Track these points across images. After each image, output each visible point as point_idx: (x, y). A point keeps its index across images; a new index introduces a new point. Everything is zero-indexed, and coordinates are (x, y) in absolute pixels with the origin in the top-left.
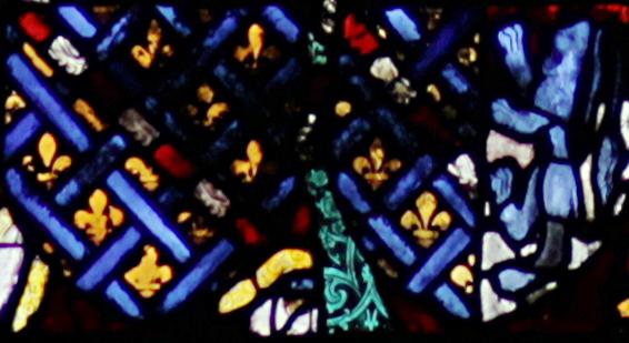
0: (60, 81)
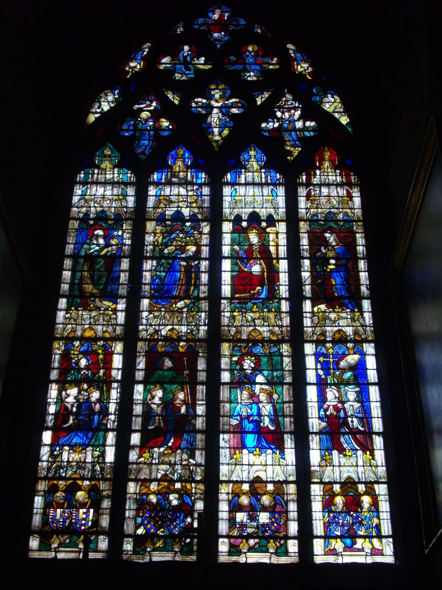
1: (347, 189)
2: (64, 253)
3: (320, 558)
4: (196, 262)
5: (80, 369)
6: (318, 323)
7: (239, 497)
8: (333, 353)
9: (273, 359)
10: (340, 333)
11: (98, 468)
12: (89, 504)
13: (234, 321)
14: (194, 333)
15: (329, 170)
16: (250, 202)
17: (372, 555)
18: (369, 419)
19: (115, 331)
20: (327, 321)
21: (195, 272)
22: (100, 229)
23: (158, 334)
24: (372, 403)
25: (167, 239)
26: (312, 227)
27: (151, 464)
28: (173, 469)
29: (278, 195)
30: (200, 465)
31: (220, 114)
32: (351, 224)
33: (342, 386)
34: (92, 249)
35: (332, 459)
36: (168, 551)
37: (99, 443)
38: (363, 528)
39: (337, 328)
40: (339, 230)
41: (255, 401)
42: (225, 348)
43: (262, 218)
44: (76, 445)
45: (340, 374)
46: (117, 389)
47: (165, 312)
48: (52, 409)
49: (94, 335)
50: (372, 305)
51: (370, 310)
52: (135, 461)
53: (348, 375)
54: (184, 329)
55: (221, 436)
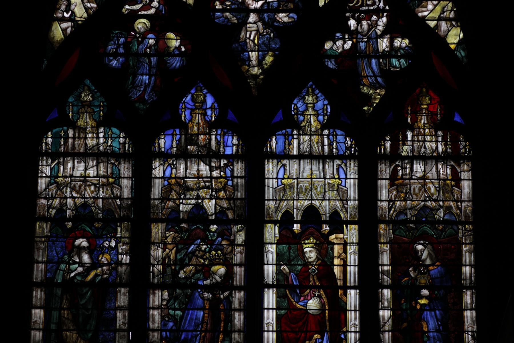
1: (452, 166)
2: (32, 278)
4: (226, 294)
15: (427, 131)
16: (306, 189)
21: (224, 310)
22: (83, 238)
25: (183, 253)
26: (397, 233)
29: (348, 177)
31: (260, 24)
32: (455, 228)
34: (72, 272)
40: (437, 238)
43: (323, 217)
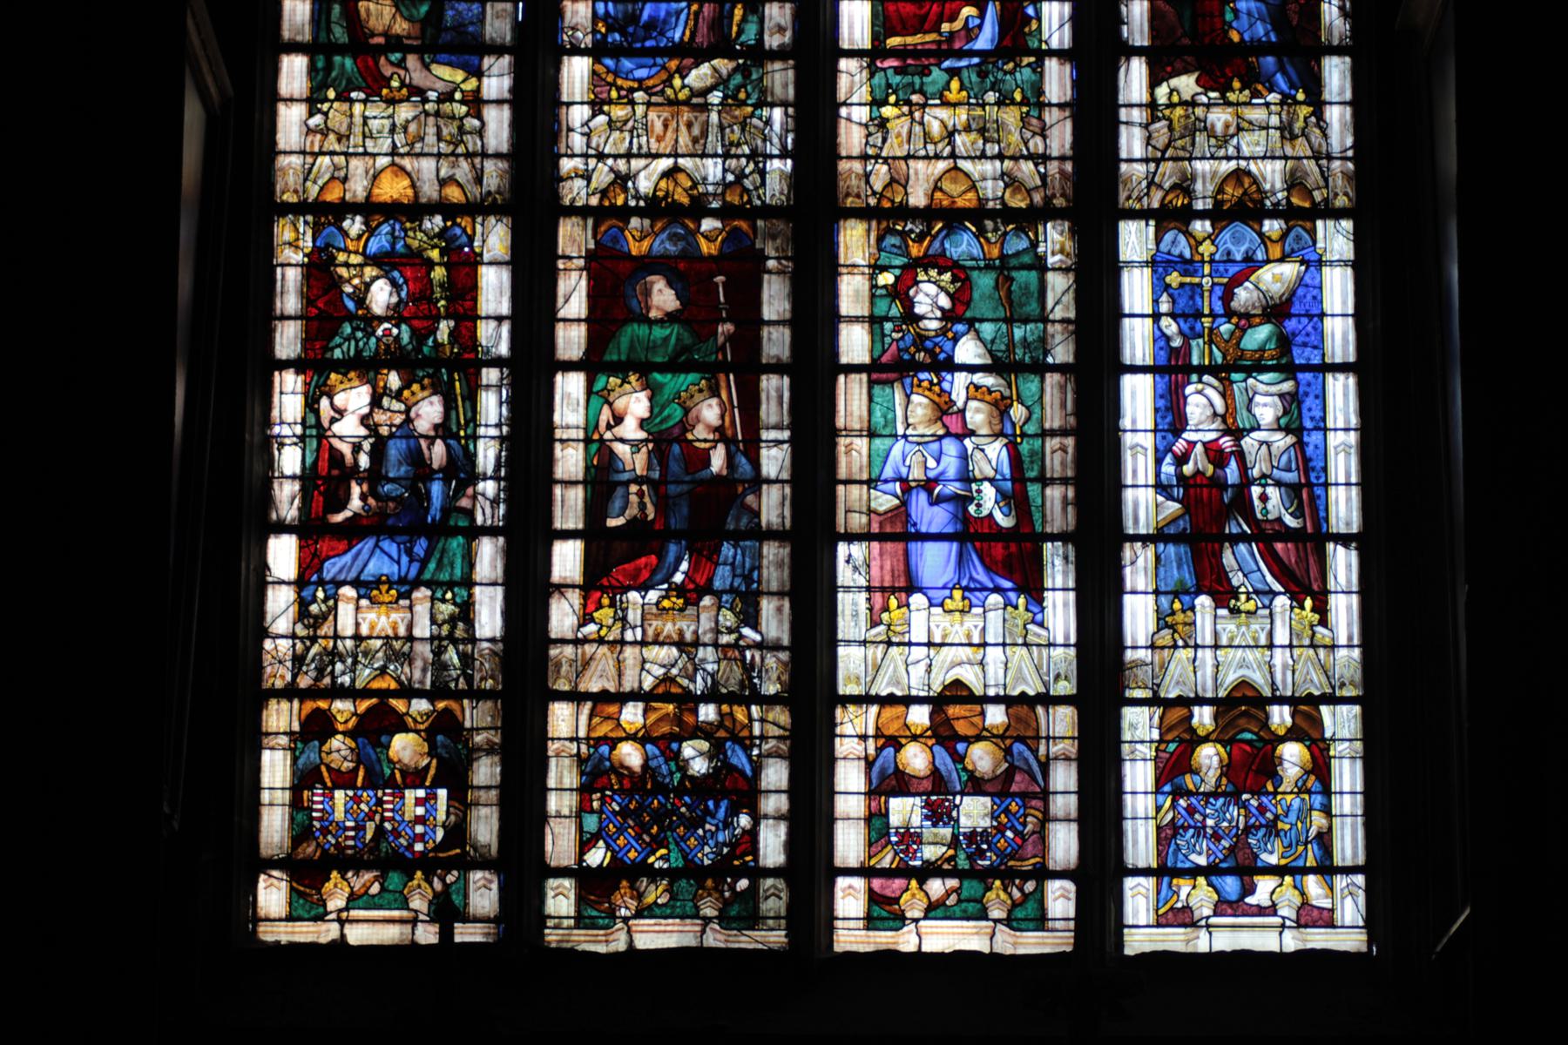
0: (614, 813)
3: (1143, 932)
5: (371, 321)
6: (1168, 146)
7: (898, 747)
8: (1212, 255)
9: (1012, 279)
10: (1240, 183)
11: (452, 656)
12: (432, 771)
13: (884, 140)
14: (747, 183)
17: (1300, 925)
18: (1319, 491)
19: (479, 180)
20: (1200, 138)
23: (625, 190)
24: (1330, 435)
27: (622, 642)
28: (691, 659)
30: (776, 647)
33: (1235, 376)
35: (1194, 623)
36: (682, 917)
37: (452, 574)
38: (1278, 843)
39: (1233, 164)
41: (953, 430)
42: (854, 241)
44: (377, 582)
45: (1232, 333)
46: (499, 387)
47: (649, 104)
48: (290, 460)
49: (410, 192)
50: (1358, 77)
51: (1348, 96)
52: (570, 636)
53: (1260, 335)
54: (713, 169)
55: (842, 549)
